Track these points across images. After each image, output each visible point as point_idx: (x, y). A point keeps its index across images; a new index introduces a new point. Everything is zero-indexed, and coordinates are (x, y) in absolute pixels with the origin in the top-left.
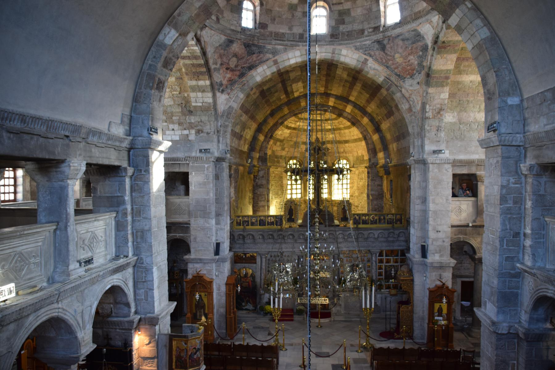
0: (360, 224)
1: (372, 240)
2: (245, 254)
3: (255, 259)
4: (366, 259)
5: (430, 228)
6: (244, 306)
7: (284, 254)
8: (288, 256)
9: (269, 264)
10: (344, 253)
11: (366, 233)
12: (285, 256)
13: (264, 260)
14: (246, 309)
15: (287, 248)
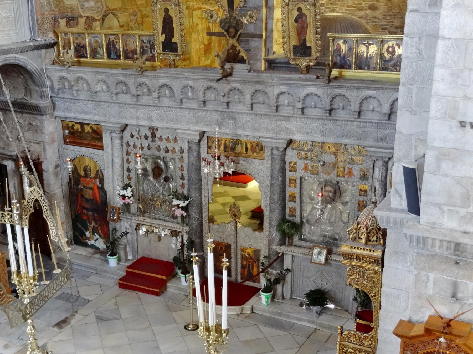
0: (350, 67)
1: (375, 117)
2: (82, 125)
3: (100, 139)
4: (356, 171)
5: (435, 108)
6: (89, 239)
7: (158, 135)
8: (168, 140)
9: (128, 153)
10: (300, 149)
11: (355, 96)
12: (161, 138)
13: (117, 142)
14: (92, 246)
15: (162, 120)
